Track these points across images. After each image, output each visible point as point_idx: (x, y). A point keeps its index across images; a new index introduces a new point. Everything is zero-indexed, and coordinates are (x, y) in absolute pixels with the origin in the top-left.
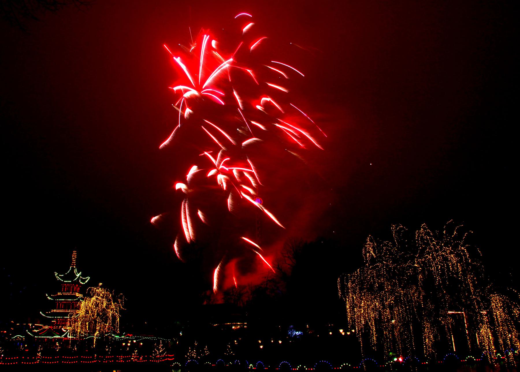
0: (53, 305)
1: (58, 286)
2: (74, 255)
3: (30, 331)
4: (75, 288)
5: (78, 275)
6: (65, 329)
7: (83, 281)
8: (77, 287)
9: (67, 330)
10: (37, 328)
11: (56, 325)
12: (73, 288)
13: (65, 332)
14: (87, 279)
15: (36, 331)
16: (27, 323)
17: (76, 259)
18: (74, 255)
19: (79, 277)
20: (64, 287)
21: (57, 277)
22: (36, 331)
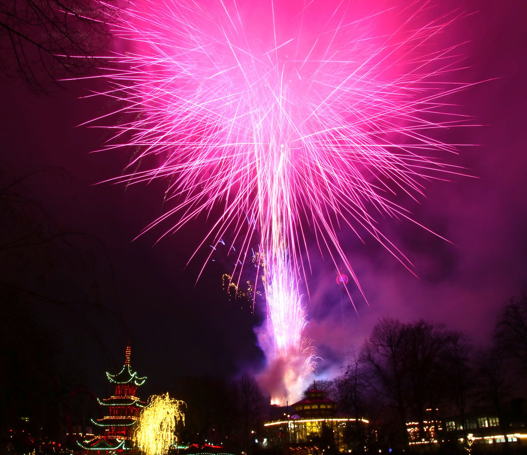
0: (106, 411)
1: (111, 389)
2: (128, 352)
3: (81, 440)
4: (130, 390)
5: (133, 375)
6: (119, 440)
7: (139, 381)
8: (133, 390)
9: (122, 440)
10: (89, 438)
11: (111, 435)
12: (128, 391)
13: (120, 443)
14: (142, 380)
15: (87, 442)
16: (78, 433)
17: (131, 356)
18: (128, 352)
19: (134, 379)
20: (118, 390)
21: (109, 378)
22: (87, 442)
